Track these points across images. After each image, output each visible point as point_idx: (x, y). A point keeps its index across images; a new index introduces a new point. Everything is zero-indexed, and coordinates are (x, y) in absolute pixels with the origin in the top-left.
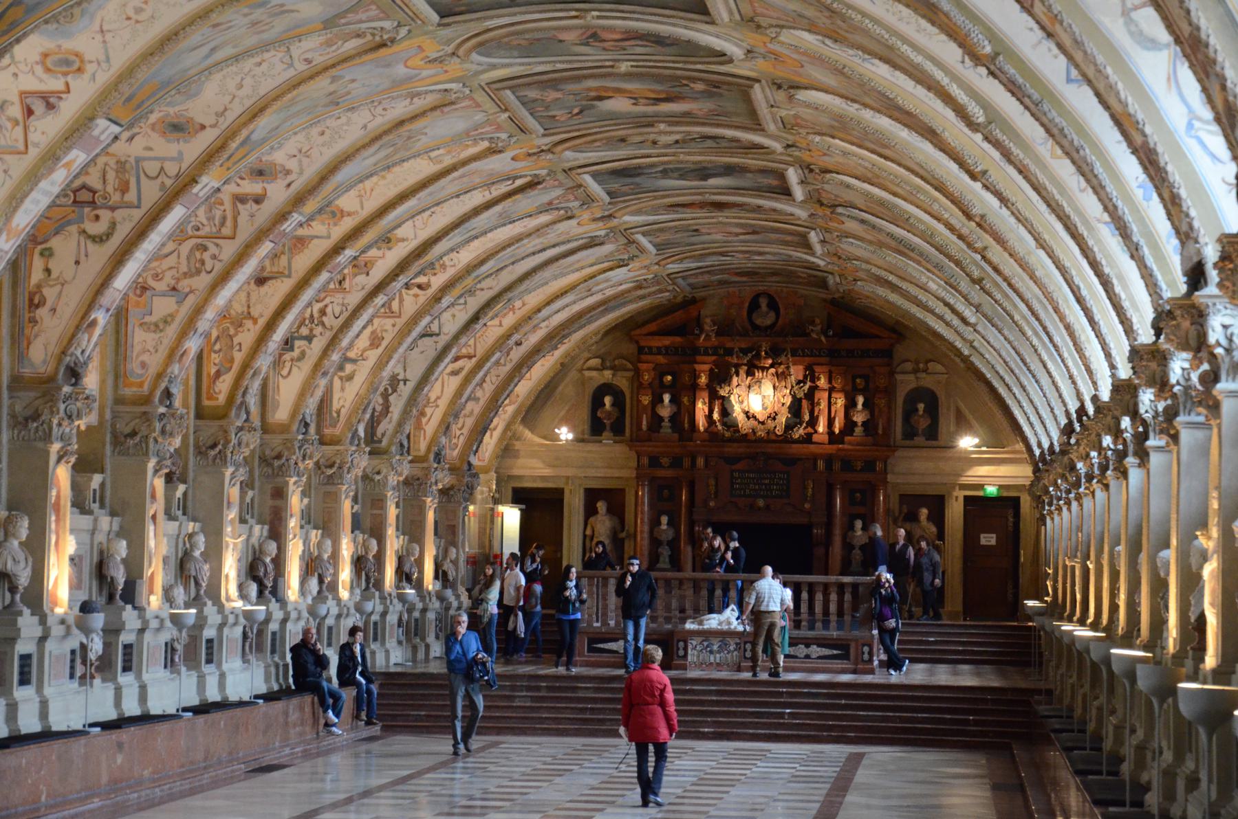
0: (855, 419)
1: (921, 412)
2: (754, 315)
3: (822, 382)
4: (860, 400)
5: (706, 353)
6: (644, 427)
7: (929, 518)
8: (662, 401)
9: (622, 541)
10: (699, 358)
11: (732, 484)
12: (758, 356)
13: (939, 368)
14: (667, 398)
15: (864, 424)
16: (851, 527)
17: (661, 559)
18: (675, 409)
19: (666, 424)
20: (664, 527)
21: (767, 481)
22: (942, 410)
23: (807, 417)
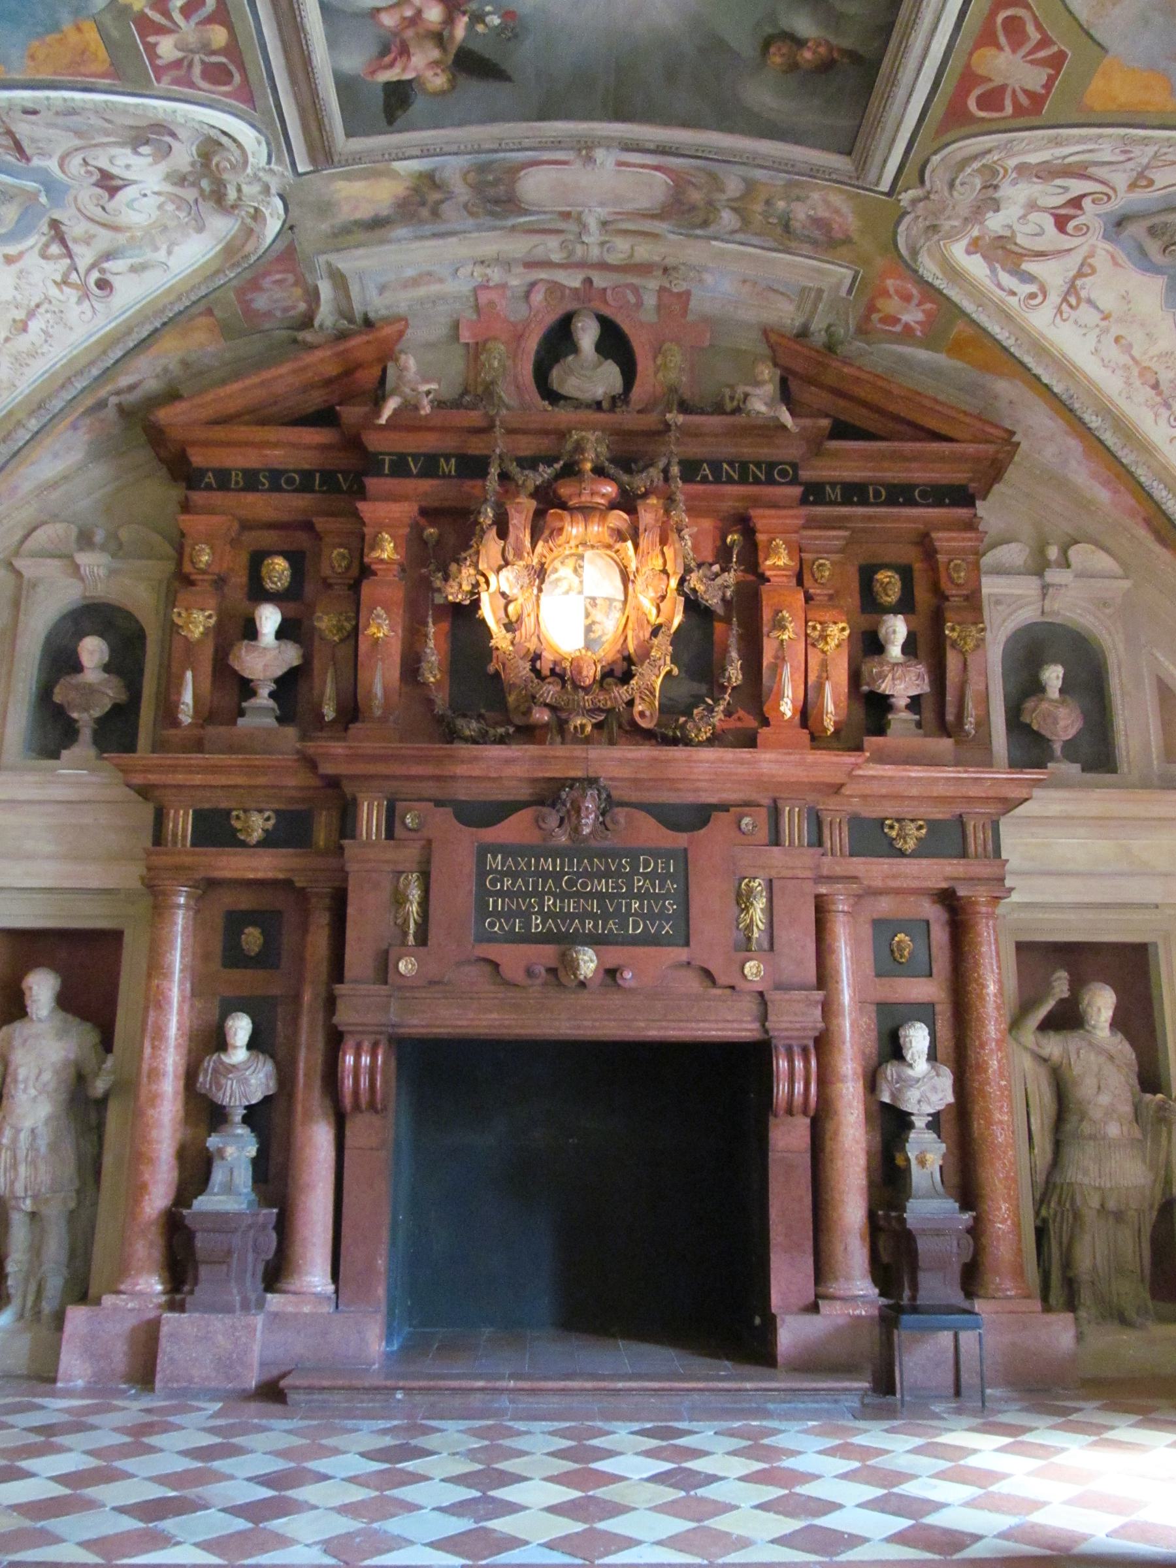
0: (885, 687)
1: (1053, 692)
2: (555, 373)
3: (778, 561)
4: (897, 629)
5: (400, 468)
6: (186, 715)
7: (1117, 1024)
8: (251, 632)
9: (102, 1103)
10: (372, 483)
11: (482, 894)
12: (571, 471)
13: (1103, 561)
14: (269, 619)
15: (915, 703)
16: (893, 1049)
17: (218, 1176)
18: (291, 655)
19: (263, 697)
20: (239, 1054)
21: (602, 886)
22: (1116, 684)
23: (735, 673)
